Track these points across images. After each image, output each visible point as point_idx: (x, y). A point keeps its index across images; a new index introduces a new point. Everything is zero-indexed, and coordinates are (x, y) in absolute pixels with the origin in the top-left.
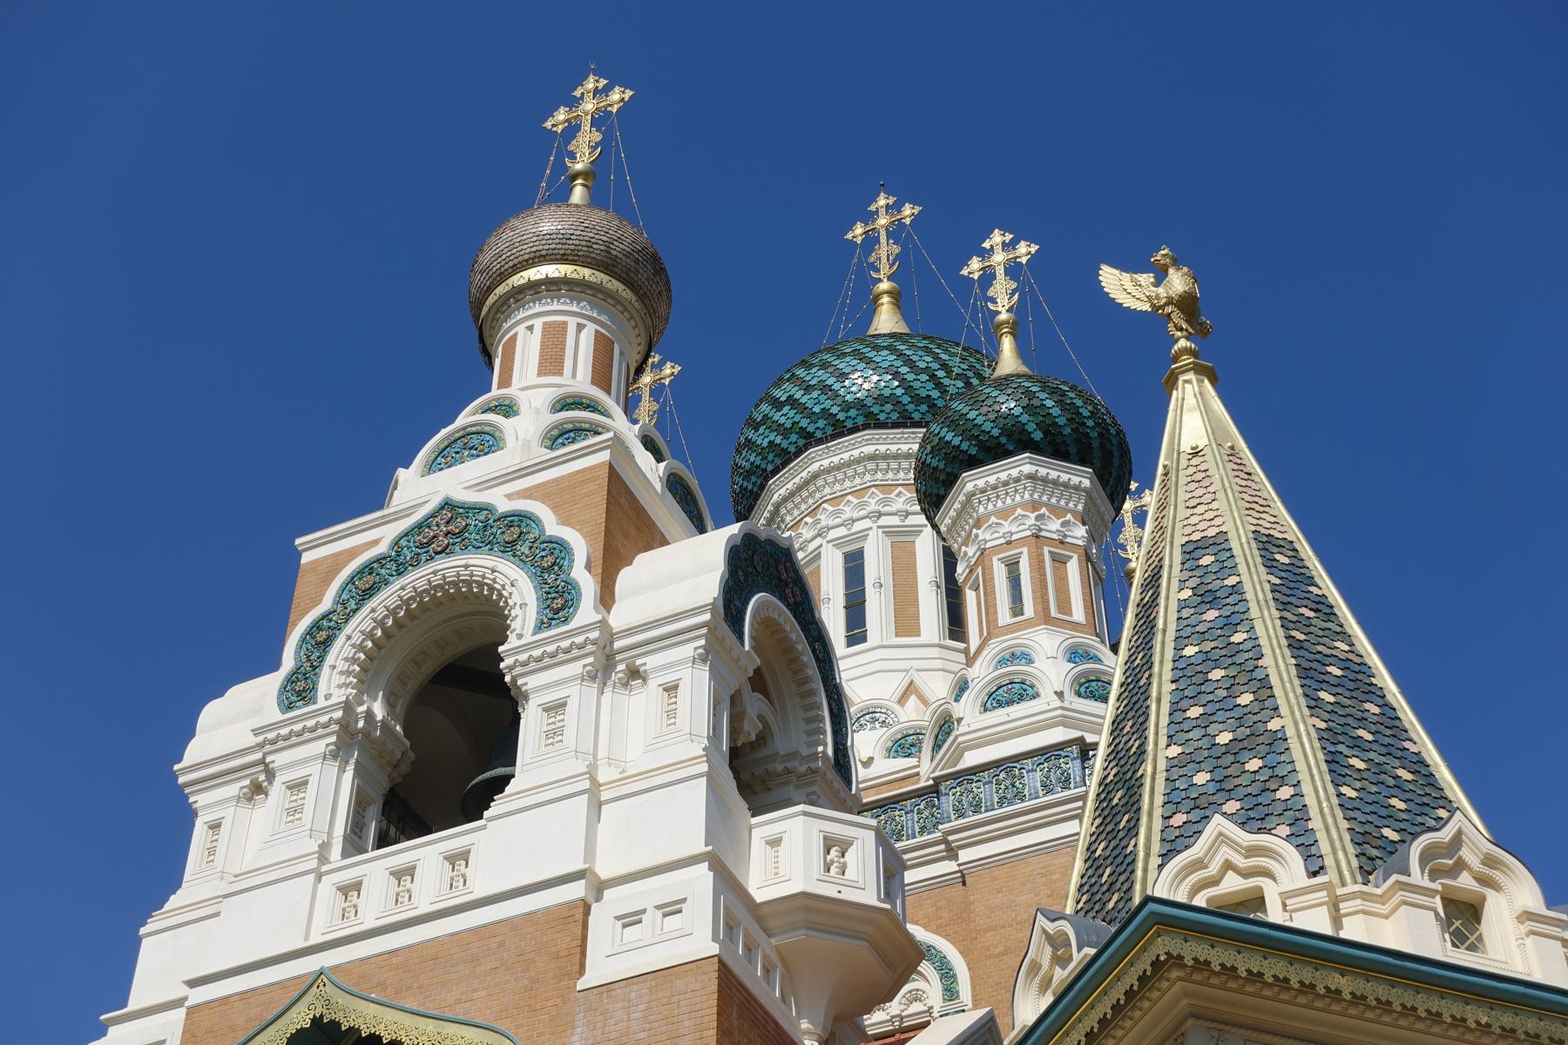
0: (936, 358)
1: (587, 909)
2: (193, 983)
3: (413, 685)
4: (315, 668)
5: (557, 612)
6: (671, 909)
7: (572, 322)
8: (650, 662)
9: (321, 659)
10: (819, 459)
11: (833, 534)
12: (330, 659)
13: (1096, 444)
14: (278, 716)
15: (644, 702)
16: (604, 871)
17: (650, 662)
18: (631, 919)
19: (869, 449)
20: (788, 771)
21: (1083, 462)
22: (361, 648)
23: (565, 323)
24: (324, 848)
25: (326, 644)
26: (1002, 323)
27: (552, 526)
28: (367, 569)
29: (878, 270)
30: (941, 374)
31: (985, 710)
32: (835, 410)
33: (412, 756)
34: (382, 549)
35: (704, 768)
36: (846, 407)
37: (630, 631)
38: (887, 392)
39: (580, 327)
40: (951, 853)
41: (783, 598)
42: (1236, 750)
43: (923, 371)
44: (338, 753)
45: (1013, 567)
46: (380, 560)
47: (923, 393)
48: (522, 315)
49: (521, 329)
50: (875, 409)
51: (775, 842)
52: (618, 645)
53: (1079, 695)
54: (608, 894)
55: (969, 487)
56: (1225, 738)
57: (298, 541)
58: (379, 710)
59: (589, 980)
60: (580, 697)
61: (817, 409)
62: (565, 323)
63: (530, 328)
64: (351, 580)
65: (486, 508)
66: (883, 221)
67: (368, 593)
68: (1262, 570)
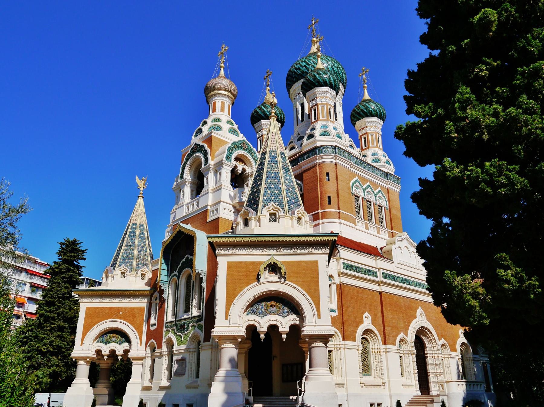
4: (183, 173)
13: (328, 82)
33: (199, 182)
34: (189, 152)
39: (219, 101)
46: (189, 154)
56: (255, 190)
59: (209, 220)
65: (199, 145)
67: (189, 159)
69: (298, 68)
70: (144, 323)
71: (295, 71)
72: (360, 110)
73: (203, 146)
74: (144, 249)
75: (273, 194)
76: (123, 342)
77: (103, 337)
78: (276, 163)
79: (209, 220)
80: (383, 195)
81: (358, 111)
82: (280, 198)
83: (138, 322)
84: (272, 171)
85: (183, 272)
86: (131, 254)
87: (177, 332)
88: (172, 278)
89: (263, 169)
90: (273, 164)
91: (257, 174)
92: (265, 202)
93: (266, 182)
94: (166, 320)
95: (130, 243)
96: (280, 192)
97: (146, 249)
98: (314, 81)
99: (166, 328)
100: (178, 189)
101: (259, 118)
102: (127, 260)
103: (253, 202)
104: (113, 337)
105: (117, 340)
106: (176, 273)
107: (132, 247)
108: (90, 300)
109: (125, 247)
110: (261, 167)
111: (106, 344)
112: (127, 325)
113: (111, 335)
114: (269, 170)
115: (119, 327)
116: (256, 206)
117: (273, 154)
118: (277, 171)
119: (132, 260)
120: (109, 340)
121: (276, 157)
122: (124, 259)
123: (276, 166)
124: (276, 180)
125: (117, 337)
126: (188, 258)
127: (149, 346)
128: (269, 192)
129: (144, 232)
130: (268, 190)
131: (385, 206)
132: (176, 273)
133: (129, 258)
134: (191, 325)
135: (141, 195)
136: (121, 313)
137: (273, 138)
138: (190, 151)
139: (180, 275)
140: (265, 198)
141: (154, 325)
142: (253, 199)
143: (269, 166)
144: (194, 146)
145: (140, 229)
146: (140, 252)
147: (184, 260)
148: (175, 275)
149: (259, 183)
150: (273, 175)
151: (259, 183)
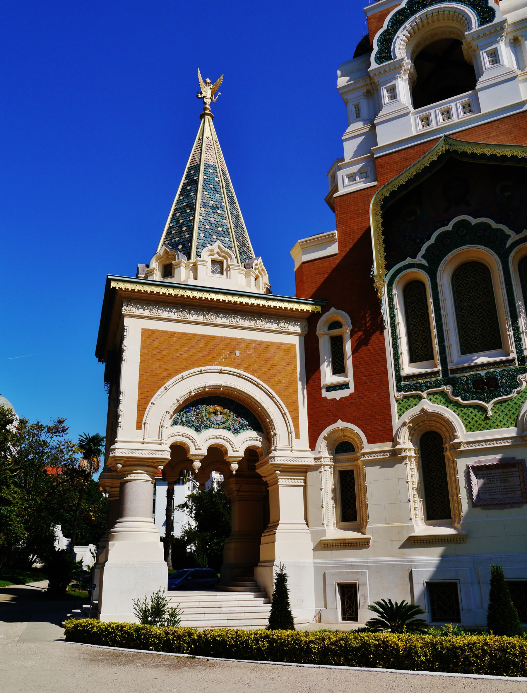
3: (415, 55)
28: (399, 13)
46: (403, 10)
70: (299, 384)
76: (242, 427)
77: (189, 412)
85: (450, 255)
87: (459, 398)
100: (361, 87)
104: (215, 413)
105: (227, 420)
107: (219, 212)
108: (154, 311)
109: (203, 209)
111: (198, 429)
112: (257, 386)
113: (211, 408)
120: (205, 419)
122: (208, 234)
125: (226, 414)
127: (325, 438)
132: (419, 259)
136: (238, 353)
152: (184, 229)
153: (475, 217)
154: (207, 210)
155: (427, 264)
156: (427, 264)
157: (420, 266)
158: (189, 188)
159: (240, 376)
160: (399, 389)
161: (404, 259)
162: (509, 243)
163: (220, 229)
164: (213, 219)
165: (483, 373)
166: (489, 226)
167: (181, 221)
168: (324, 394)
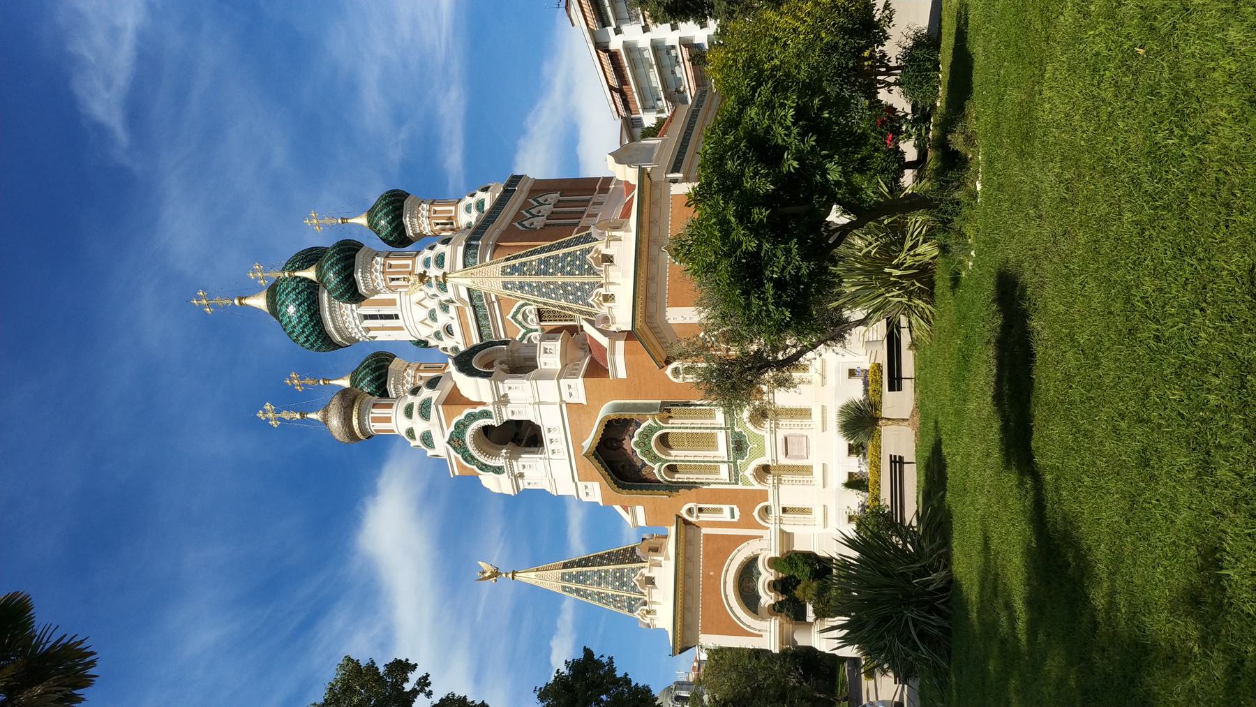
0: (290, 292)
1: (567, 404)
2: (574, 480)
5: (487, 415)
6: (570, 387)
7: (371, 415)
8: (502, 393)
9: (490, 466)
10: (330, 327)
11: (357, 322)
12: (491, 464)
14: (506, 474)
15: (511, 395)
16: (558, 400)
17: (502, 393)
18: (571, 394)
19: (327, 313)
20: (511, 357)
21: (354, 257)
22: (489, 457)
23: (372, 417)
24: (541, 459)
25: (485, 465)
26: (289, 275)
27: (462, 417)
28: (465, 459)
29: (228, 304)
30: (297, 291)
31: (447, 291)
32: (312, 324)
34: (459, 456)
35: (534, 381)
36: (311, 320)
37: (494, 398)
38: (306, 308)
39: (372, 413)
40: (493, 302)
41: (471, 359)
42: (565, 290)
43: (297, 297)
44: (517, 459)
45: (393, 279)
46: (462, 456)
47: (306, 296)
48: (368, 427)
49: (373, 429)
50: (312, 311)
51: (545, 364)
52: (497, 400)
53: (443, 267)
54: (563, 399)
55: (364, 291)
56: (561, 292)
57: (452, 476)
58: (504, 451)
59: (584, 402)
60: (510, 407)
61: (312, 329)
62: (372, 417)
63: (373, 426)
64: (467, 462)
66: (204, 302)
67: (473, 458)
68: (514, 276)
69: (297, 320)
71: (301, 325)
72: (389, 226)
73: (457, 426)
74: (607, 556)
75: (571, 263)
78: (523, 264)
79: (584, 402)
80: (540, 196)
81: (390, 229)
82: (578, 253)
83: (727, 543)
84: (536, 268)
85: (656, 452)
86: (615, 574)
88: (662, 478)
89: (530, 285)
90: (525, 269)
91: (536, 293)
92: (583, 272)
93: (552, 274)
94: (726, 484)
95: (596, 578)
96: (569, 254)
97: (606, 553)
98: (343, 275)
99: (738, 484)
101: (382, 390)
102: (625, 579)
103: (579, 294)
106: (656, 466)
107: (603, 574)
109: (603, 586)
110: (526, 288)
114: (533, 273)
115: (734, 571)
116: (587, 287)
117: (509, 270)
118: (537, 261)
119: (626, 570)
121: (514, 265)
122: (623, 584)
123: (528, 263)
124: (551, 261)
126: (636, 444)
128: (569, 268)
129: (574, 573)
130: (565, 271)
131: (558, 195)
133: (622, 575)
134: (737, 429)
135: (510, 575)
136: (711, 573)
137: (481, 273)
138: (458, 453)
139: (660, 460)
140: (577, 273)
141: (732, 511)
142: (574, 294)
143: (528, 273)
144: (451, 445)
145: (573, 567)
146: (612, 561)
147: (638, 451)
148: (659, 471)
149: (552, 286)
150: (542, 267)
151: (552, 286)
152: (618, 599)
153: (633, 437)
154: (603, 583)
155: (660, 463)
156: (660, 463)
157: (662, 465)
158: (582, 593)
159: (727, 571)
160: (737, 484)
161: (654, 474)
162: (653, 424)
163: (618, 575)
164: (610, 579)
165: (732, 446)
166: (641, 433)
167: (611, 600)
168: (736, 519)
